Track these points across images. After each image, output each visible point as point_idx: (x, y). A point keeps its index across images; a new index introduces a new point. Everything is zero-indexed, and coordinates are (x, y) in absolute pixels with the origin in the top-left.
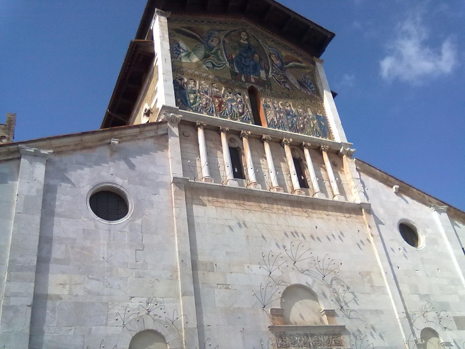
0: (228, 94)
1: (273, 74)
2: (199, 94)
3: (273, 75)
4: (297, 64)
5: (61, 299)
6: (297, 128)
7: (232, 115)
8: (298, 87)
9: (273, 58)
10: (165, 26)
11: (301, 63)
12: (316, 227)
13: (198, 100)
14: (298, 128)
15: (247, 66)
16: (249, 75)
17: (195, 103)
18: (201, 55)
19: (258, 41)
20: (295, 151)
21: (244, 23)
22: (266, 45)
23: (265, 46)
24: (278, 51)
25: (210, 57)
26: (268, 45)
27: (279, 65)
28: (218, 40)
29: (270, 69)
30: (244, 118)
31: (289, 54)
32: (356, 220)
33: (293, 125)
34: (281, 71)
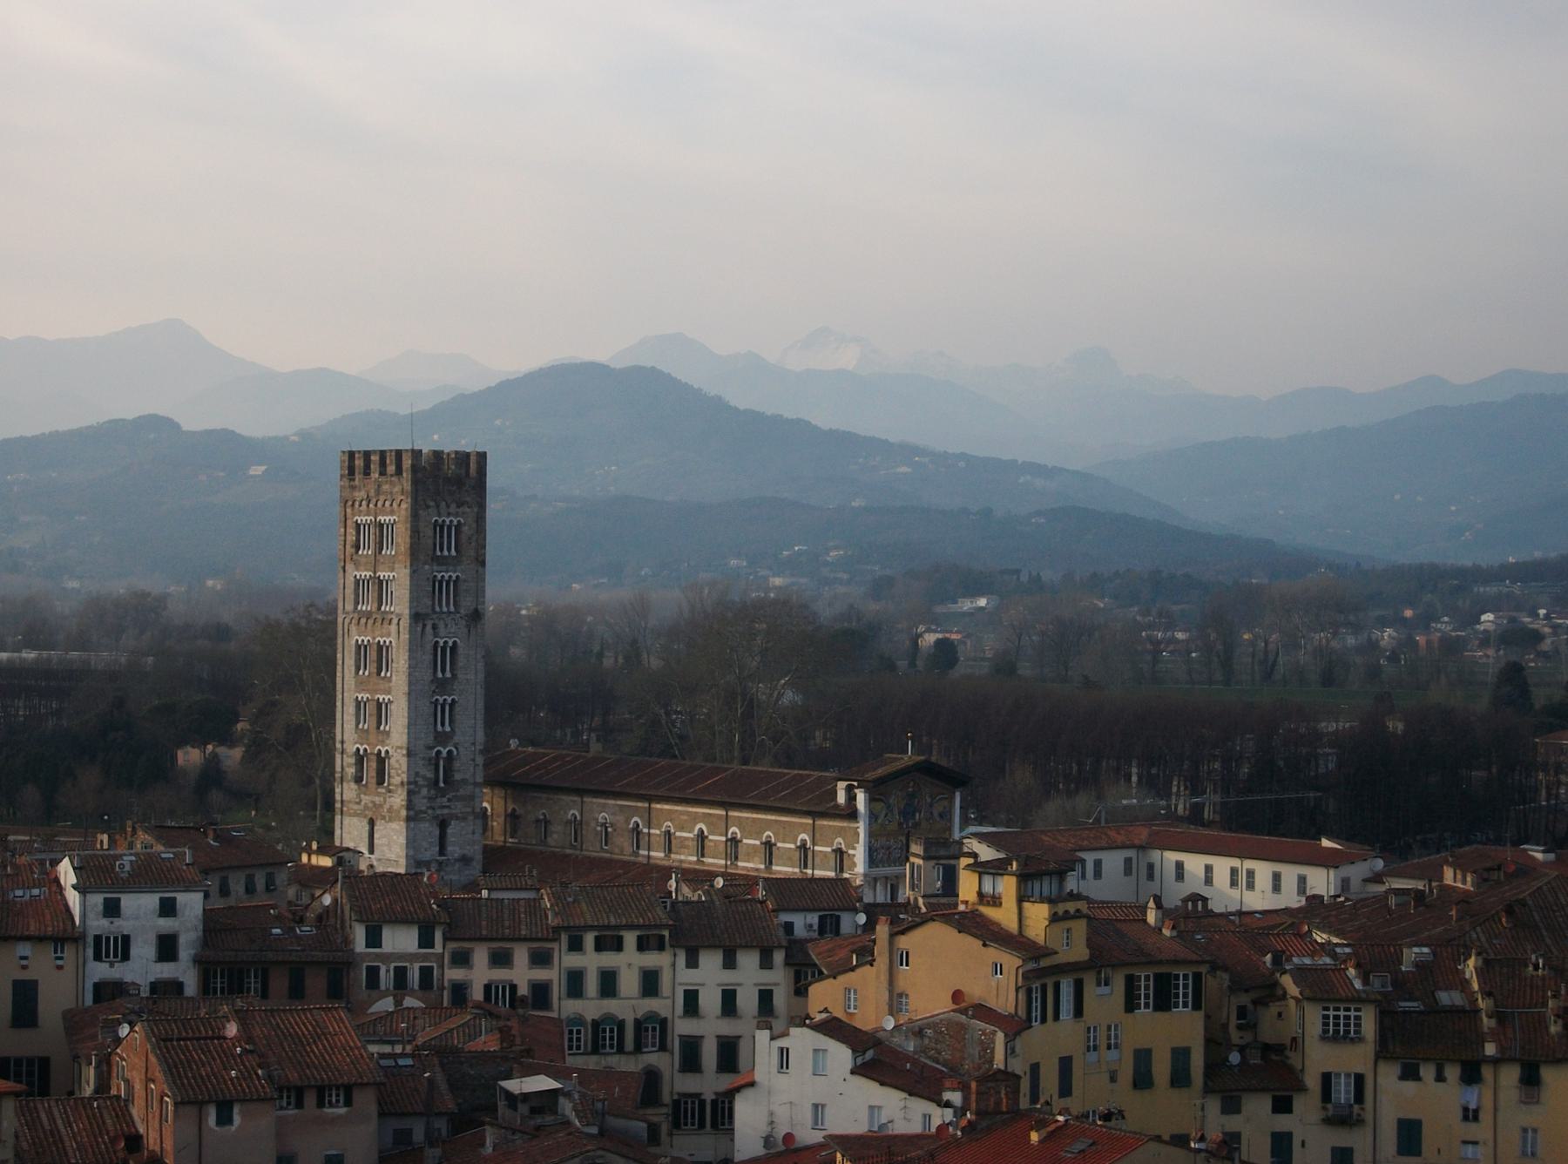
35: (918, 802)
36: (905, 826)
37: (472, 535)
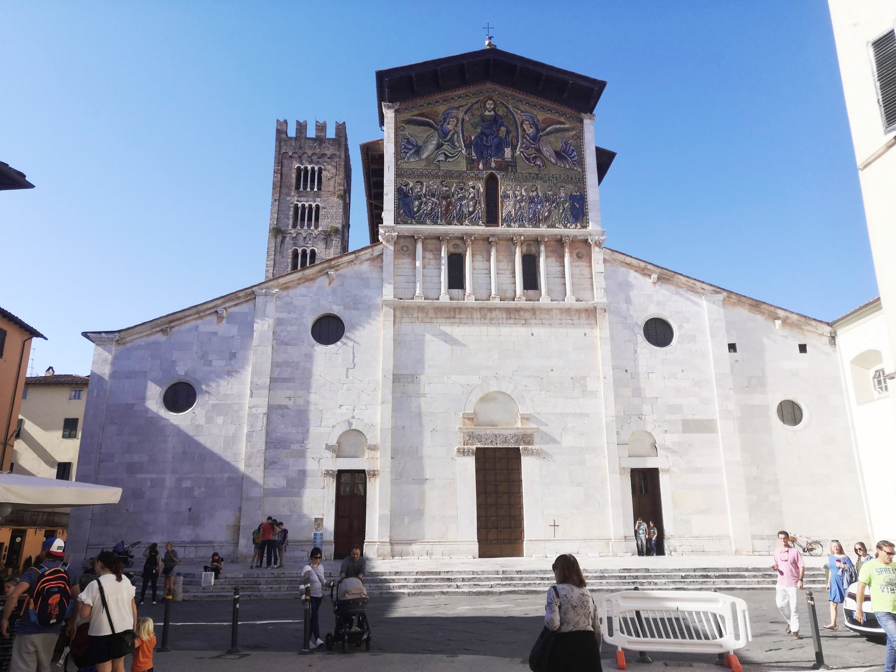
0: (459, 190)
1: (521, 150)
2: (424, 199)
3: (521, 152)
4: (558, 126)
5: (288, 408)
6: (539, 218)
8: (553, 161)
9: (525, 127)
10: (392, 122)
11: (564, 123)
12: (532, 334)
13: (422, 206)
14: (541, 218)
15: (488, 147)
16: (489, 159)
17: (418, 211)
18: (433, 146)
19: (507, 108)
21: (491, 89)
22: (517, 111)
23: (516, 113)
24: (532, 115)
25: (444, 147)
26: (520, 110)
28: (455, 120)
29: (519, 143)
33: (534, 215)
34: (534, 143)
35: (508, 132)
36: (481, 166)
37: (332, 177)
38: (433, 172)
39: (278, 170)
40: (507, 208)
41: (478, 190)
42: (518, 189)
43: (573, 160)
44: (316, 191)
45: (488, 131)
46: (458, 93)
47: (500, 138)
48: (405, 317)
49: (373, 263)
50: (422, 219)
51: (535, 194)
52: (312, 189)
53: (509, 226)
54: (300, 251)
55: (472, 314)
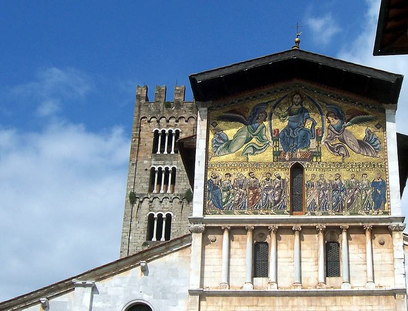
1: (326, 141)
2: (232, 190)
3: (326, 142)
4: (361, 117)
7: (265, 206)
8: (357, 150)
11: (367, 114)
13: (230, 197)
18: (243, 140)
19: (313, 101)
20: (335, 234)
21: (298, 84)
24: (336, 107)
25: (254, 140)
27: (336, 126)
28: (264, 115)
30: (279, 206)
31: (352, 107)
32: (385, 308)
33: (337, 202)
35: (314, 124)
36: (287, 157)
38: (242, 165)
39: (136, 134)
40: (311, 197)
41: (284, 180)
42: (322, 178)
43: (376, 148)
44: (173, 155)
45: (294, 125)
46: (266, 89)
47: (307, 131)
48: (210, 306)
49: (182, 254)
50: (230, 209)
51: (338, 182)
52: (169, 152)
53: (313, 214)
54: (156, 216)
55: (274, 302)
